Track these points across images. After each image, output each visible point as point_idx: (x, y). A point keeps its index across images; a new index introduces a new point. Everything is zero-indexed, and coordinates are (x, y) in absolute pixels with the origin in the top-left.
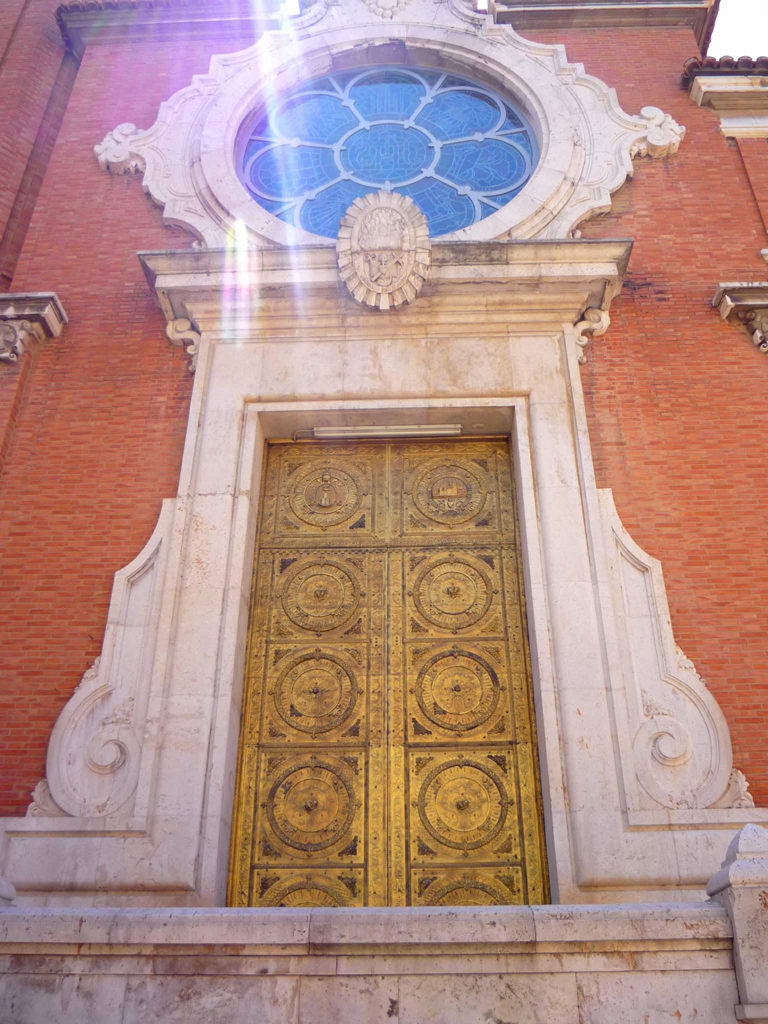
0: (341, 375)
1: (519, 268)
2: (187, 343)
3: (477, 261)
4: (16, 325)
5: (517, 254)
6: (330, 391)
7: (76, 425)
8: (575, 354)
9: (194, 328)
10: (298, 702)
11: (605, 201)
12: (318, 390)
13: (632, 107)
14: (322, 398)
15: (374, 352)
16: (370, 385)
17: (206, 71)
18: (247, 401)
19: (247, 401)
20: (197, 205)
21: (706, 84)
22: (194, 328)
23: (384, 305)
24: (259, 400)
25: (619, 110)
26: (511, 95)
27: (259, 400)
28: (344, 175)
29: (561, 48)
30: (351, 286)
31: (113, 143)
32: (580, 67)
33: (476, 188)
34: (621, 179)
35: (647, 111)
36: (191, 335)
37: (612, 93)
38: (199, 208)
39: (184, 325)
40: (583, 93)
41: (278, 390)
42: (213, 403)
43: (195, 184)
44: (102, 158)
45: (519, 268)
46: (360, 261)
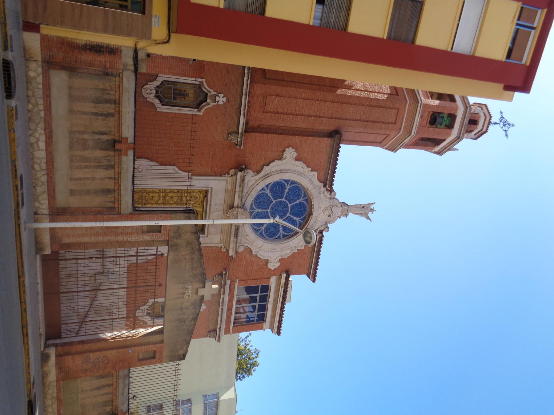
0: (215, 205)
1: (232, 239)
2: (229, 174)
3: (235, 232)
4: (236, 140)
5: (235, 239)
6: (212, 203)
7: (211, 153)
8: (217, 245)
9: (232, 176)
10: (151, 195)
11: (254, 253)
12: (212, 201)
13: (280, 260)
14: (211, 201)
15: (220, 210)
16: (212, 210)
17: (312, 170)
18: (212, 188)
19: (212, 188)
20: (267, 172)
21: (284, 276)
22: (232, 176)
23: (228, 215)
24: (212, 190)
25: (280, 258)
26: (292, 236)
27: (212, 190)
28: (274, 202)
29: (303, 248)
30: (232, 210)
31: (290, 152)
32: (296, 251)
33: (265, 228)
34: (260, 257)
35: (278, 264)
36: (230, 175)
37: (286, 257)
38: (267, 173)
39: (233, 173)
40: (288, 251)
41: (213, 193)
42: (211, 182)
43: (274, 172)
44: (287, 149)
45: (232, 239)
46: (236, 212)
